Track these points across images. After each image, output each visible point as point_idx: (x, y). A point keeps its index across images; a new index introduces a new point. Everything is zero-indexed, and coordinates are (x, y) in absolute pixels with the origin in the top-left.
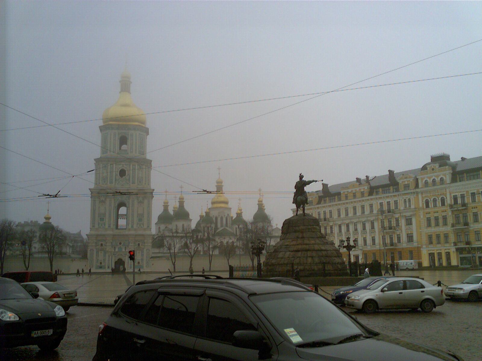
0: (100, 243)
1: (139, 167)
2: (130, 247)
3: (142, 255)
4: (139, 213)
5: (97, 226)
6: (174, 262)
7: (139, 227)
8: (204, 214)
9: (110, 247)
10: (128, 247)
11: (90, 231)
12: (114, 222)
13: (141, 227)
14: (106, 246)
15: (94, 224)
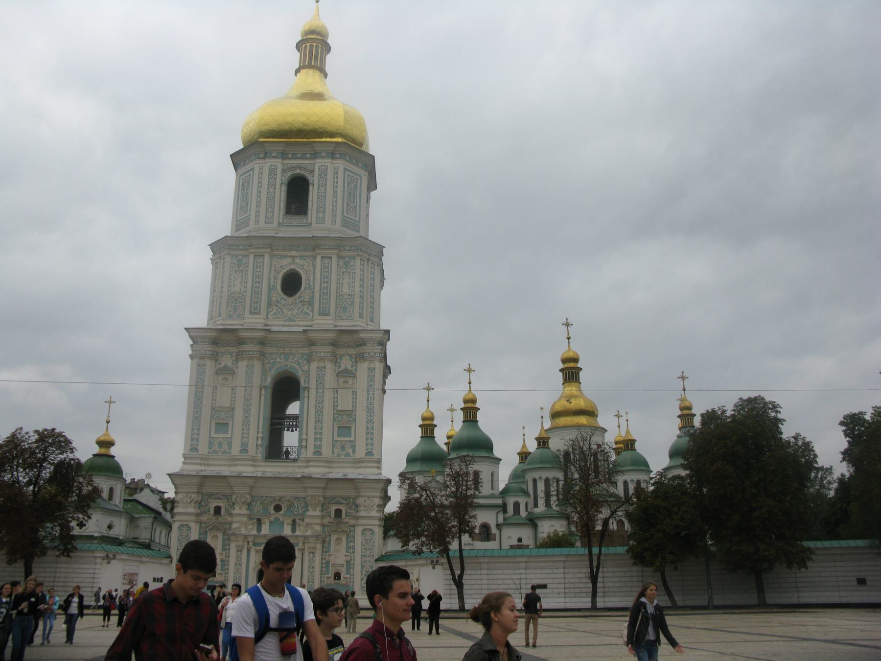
0: (213, 504)
1: (342, 264)
2: (306, 520)
3: (350, 549)
4: (339, 408)
5: (203, 448)
6: (457, 572)
7: (339, 455)
8: (532, 446)
9: (245, 519)
10: (303, 520)
11: (184, 463)
12: (260, 435)
13: (348, 455)
14: (231, 515)
15: (195, 442)
